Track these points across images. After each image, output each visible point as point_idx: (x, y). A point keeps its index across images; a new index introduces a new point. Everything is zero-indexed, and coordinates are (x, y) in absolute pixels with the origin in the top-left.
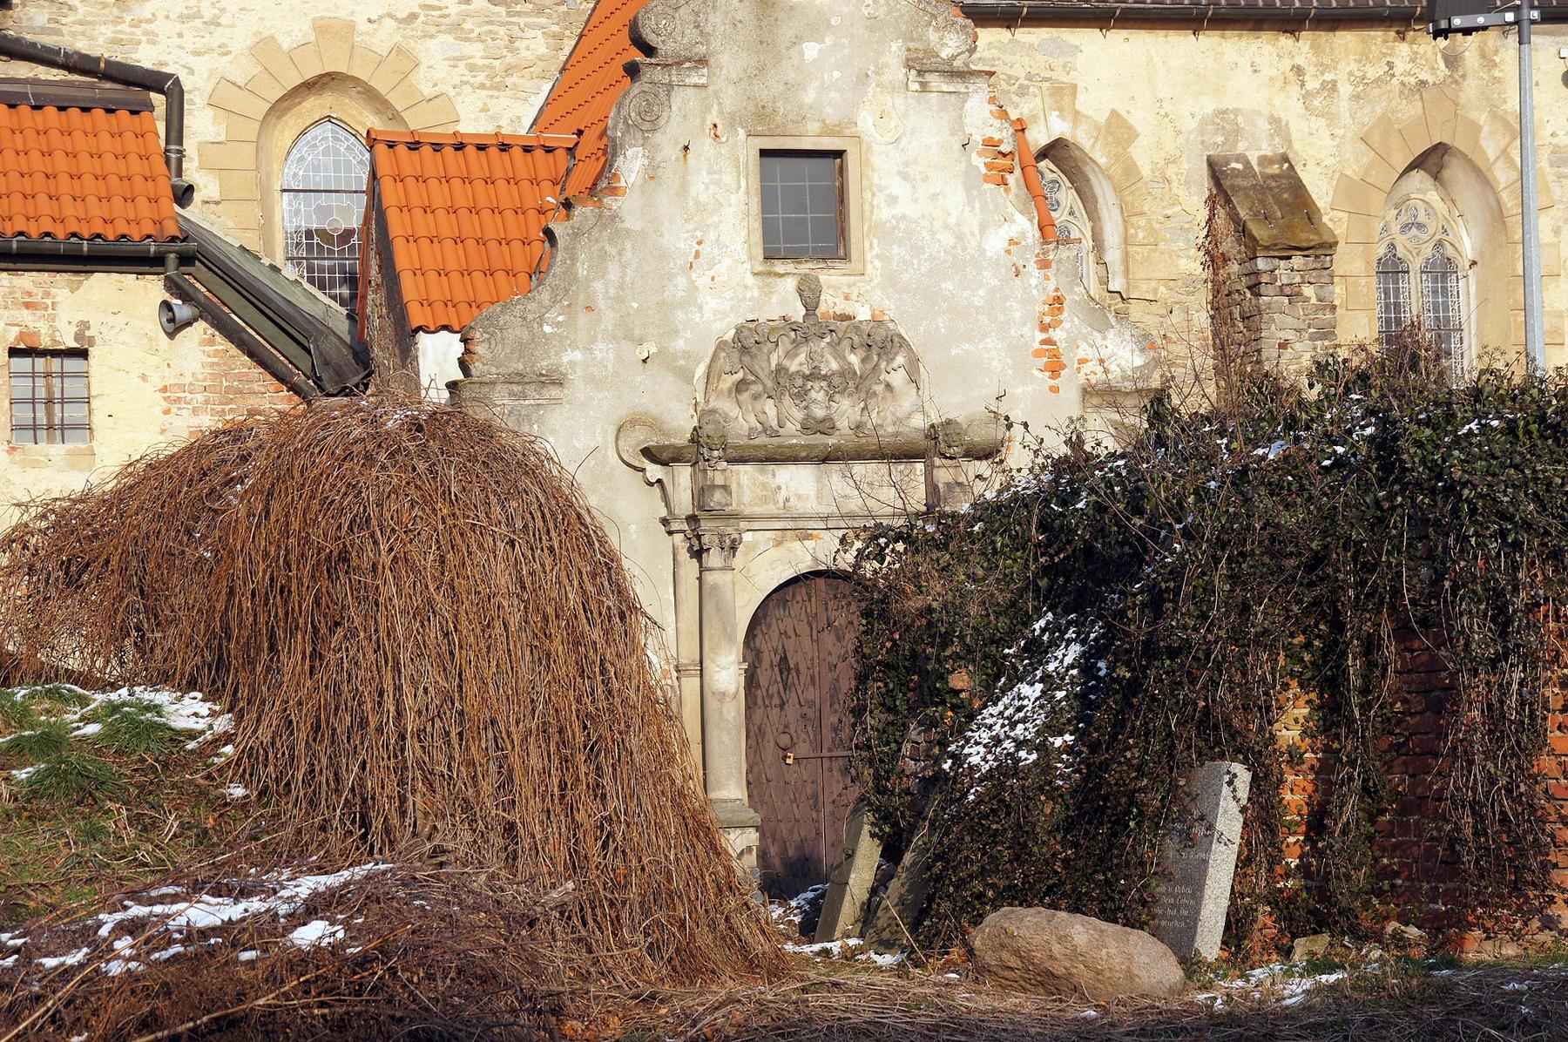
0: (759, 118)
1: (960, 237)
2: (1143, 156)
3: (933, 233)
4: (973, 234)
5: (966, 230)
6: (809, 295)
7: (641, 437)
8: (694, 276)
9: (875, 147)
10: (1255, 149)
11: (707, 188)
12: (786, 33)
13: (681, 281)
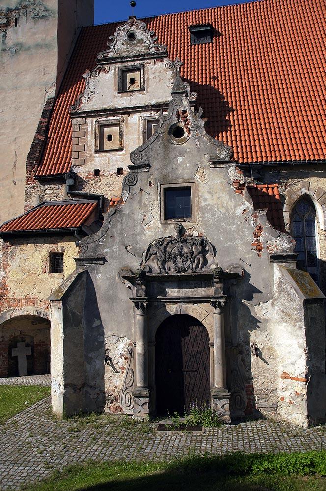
0: (164, 179)
1: (227, 210)
3: (218, 209)
4: (232, 209)
5: (229, 208)
6: (181, 231)
7: (124, 274)
8: (143, 225)
9: (200, 185)
11: (148, 200)
12: (173, 155)
13: (139, 227)
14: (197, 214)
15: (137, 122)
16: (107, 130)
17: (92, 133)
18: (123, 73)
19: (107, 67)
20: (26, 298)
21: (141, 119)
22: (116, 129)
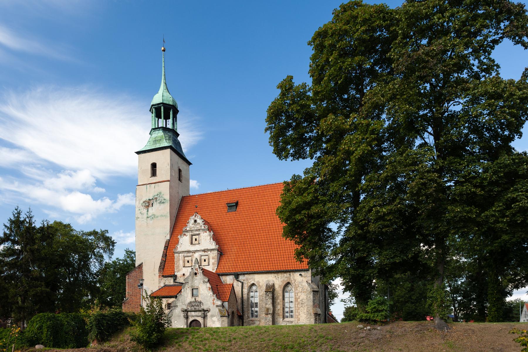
0: (192, 286)
2: (261, 284)
6: (195, 299)
10: (271, 283)
14: (200, 296)
16: (187, 259)
18: (192, 235)
19: (187, 234)
22: (190, 258)
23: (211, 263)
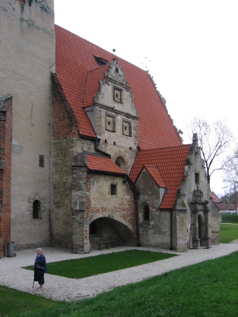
15: (120, 119)
17: (104, 118)
19: (109, 83)
20: (102, 208)
21: (122, 119)
23: (133, 135)
